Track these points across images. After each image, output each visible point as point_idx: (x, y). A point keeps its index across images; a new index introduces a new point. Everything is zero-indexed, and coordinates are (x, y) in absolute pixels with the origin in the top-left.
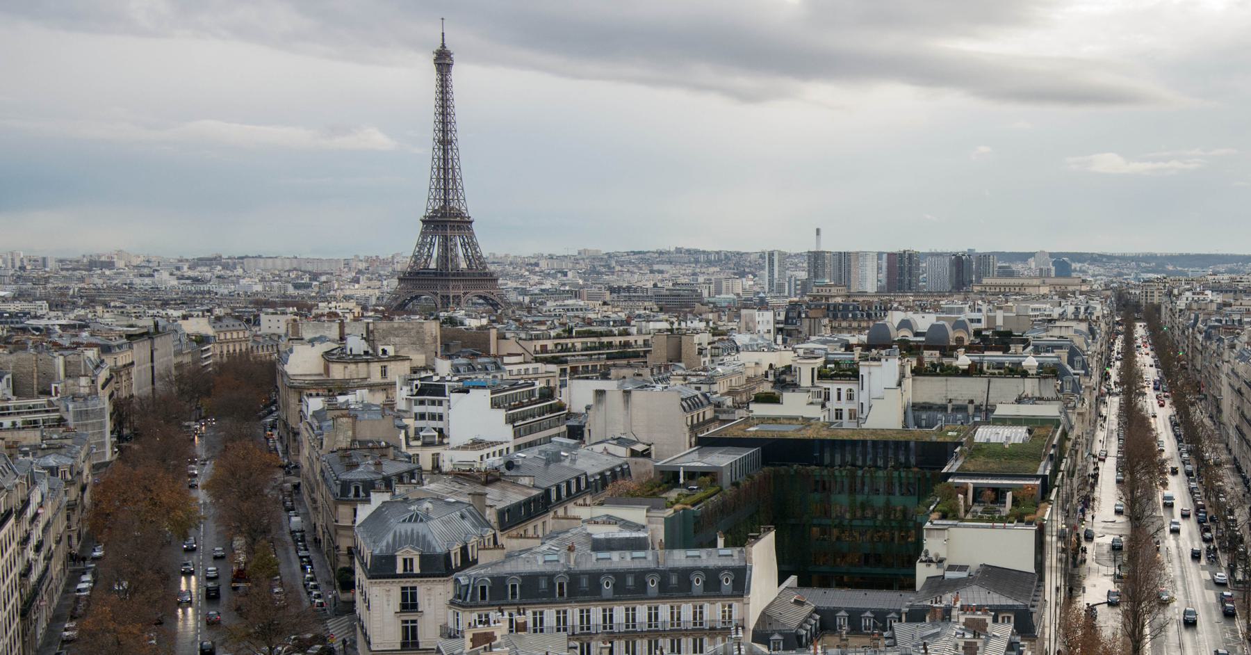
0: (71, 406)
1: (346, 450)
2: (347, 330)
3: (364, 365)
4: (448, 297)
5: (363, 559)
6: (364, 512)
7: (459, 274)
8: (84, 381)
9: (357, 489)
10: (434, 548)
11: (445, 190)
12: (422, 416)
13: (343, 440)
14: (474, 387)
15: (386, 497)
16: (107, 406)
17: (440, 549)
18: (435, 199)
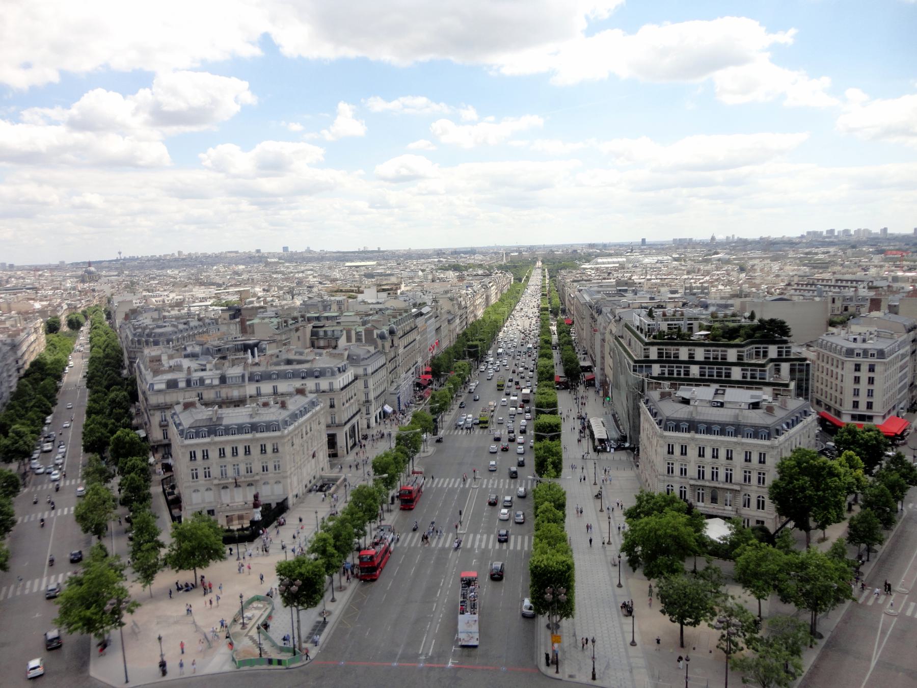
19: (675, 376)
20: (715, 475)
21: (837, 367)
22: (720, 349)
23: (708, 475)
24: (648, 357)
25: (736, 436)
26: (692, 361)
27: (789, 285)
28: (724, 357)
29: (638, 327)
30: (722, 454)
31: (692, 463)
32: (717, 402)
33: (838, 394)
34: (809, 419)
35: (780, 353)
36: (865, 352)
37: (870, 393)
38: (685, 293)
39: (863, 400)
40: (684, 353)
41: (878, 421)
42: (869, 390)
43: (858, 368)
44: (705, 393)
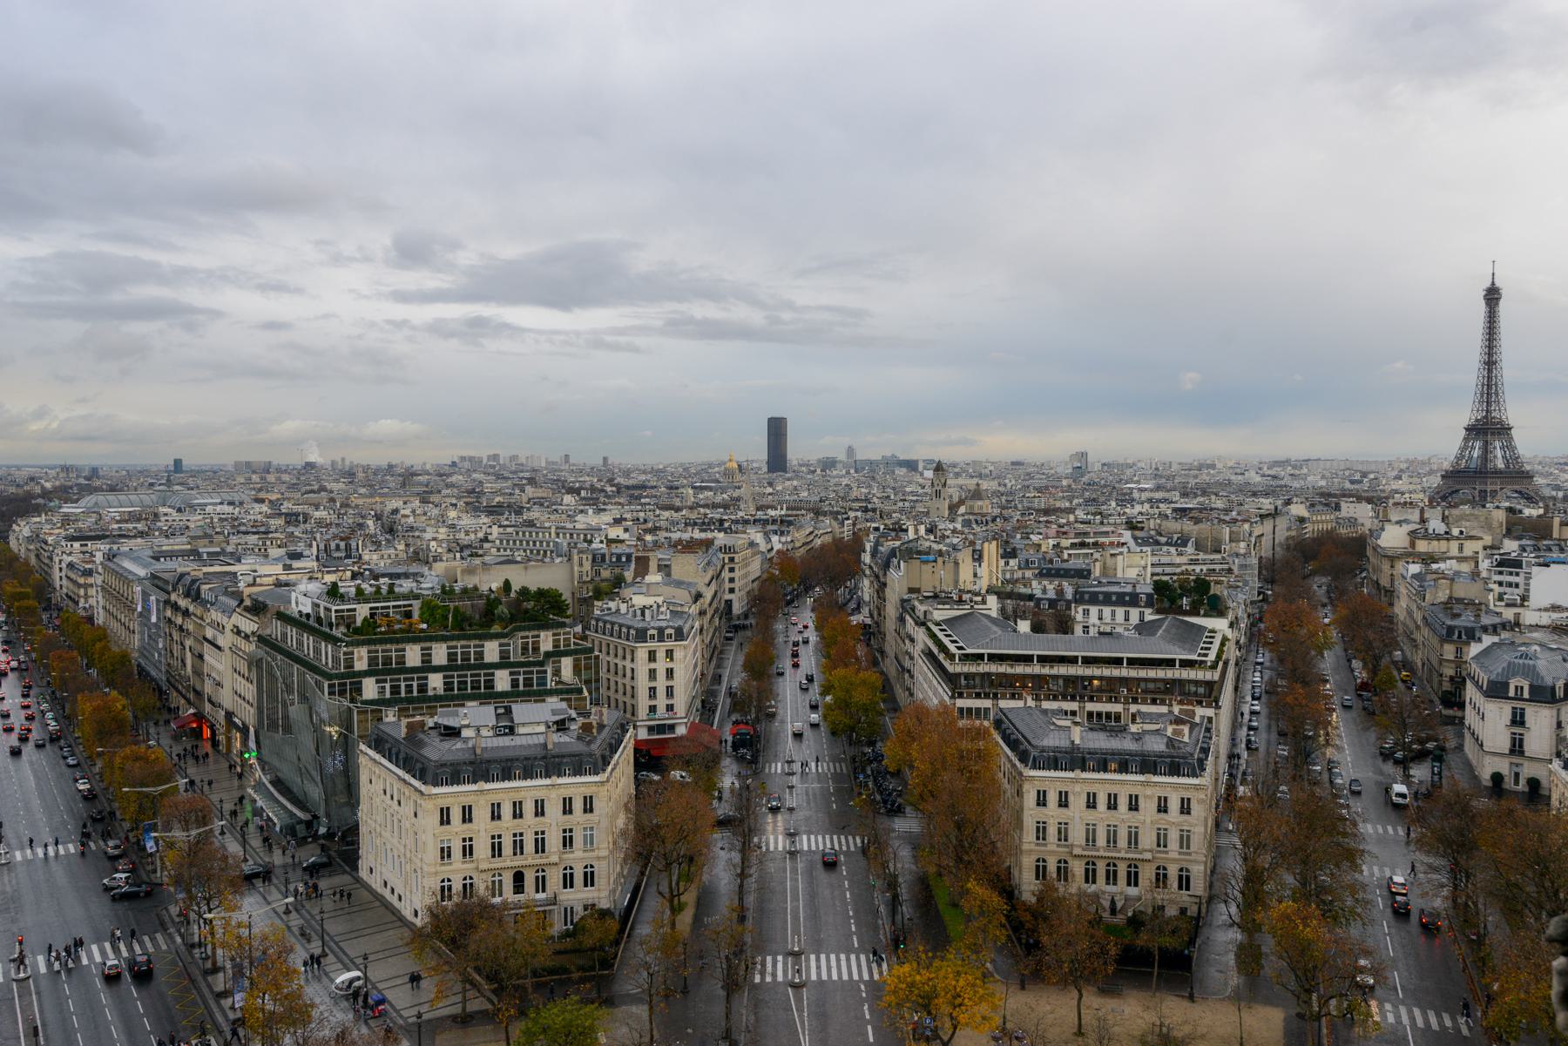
0: (1236, 561)
1: (1446, 603)
2: (1426, 515)
3: (1445, 542)
4: (1485, 491)
5: (1478, 682)
6: (1475, 649)
7: (1497, 473)
8: (1243, 545)
9: (1460, 633)
10: (1542, 678)
11: (1487, 402)
12: (1500, 584)
13: (1442, 596)
14: (1554, 562)
15: (1496, 639)
16: (1255, 561)
17: (1549, 681)
18: (1478, 411)
19: (403, 695)
20: (518, 847)
21: (624, 658)
22: (472, 643)
23: (507, 848)
24: (353, 667)
25: (548, 776)
26: (427, 667)
27: (486, 540)
28: (480, 655)
29: (308, 616)
30: (529, 808)
31: (482, 833)
32: (505, 727)
33: (628, 699)
34: (628, 735)
35: (556, 644)
36: (661, 630)
37: (670, 692)
38: (317, 557)
39: (661, 701)
40: (413, 656)
41: (681, 731)
42: (667, 687)
43: (652, 656)
44: (475, 719)
